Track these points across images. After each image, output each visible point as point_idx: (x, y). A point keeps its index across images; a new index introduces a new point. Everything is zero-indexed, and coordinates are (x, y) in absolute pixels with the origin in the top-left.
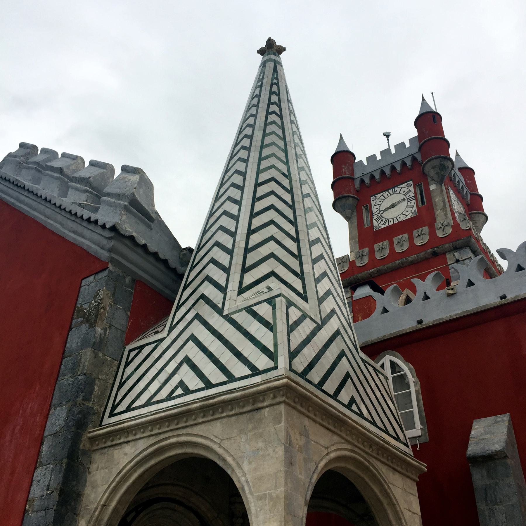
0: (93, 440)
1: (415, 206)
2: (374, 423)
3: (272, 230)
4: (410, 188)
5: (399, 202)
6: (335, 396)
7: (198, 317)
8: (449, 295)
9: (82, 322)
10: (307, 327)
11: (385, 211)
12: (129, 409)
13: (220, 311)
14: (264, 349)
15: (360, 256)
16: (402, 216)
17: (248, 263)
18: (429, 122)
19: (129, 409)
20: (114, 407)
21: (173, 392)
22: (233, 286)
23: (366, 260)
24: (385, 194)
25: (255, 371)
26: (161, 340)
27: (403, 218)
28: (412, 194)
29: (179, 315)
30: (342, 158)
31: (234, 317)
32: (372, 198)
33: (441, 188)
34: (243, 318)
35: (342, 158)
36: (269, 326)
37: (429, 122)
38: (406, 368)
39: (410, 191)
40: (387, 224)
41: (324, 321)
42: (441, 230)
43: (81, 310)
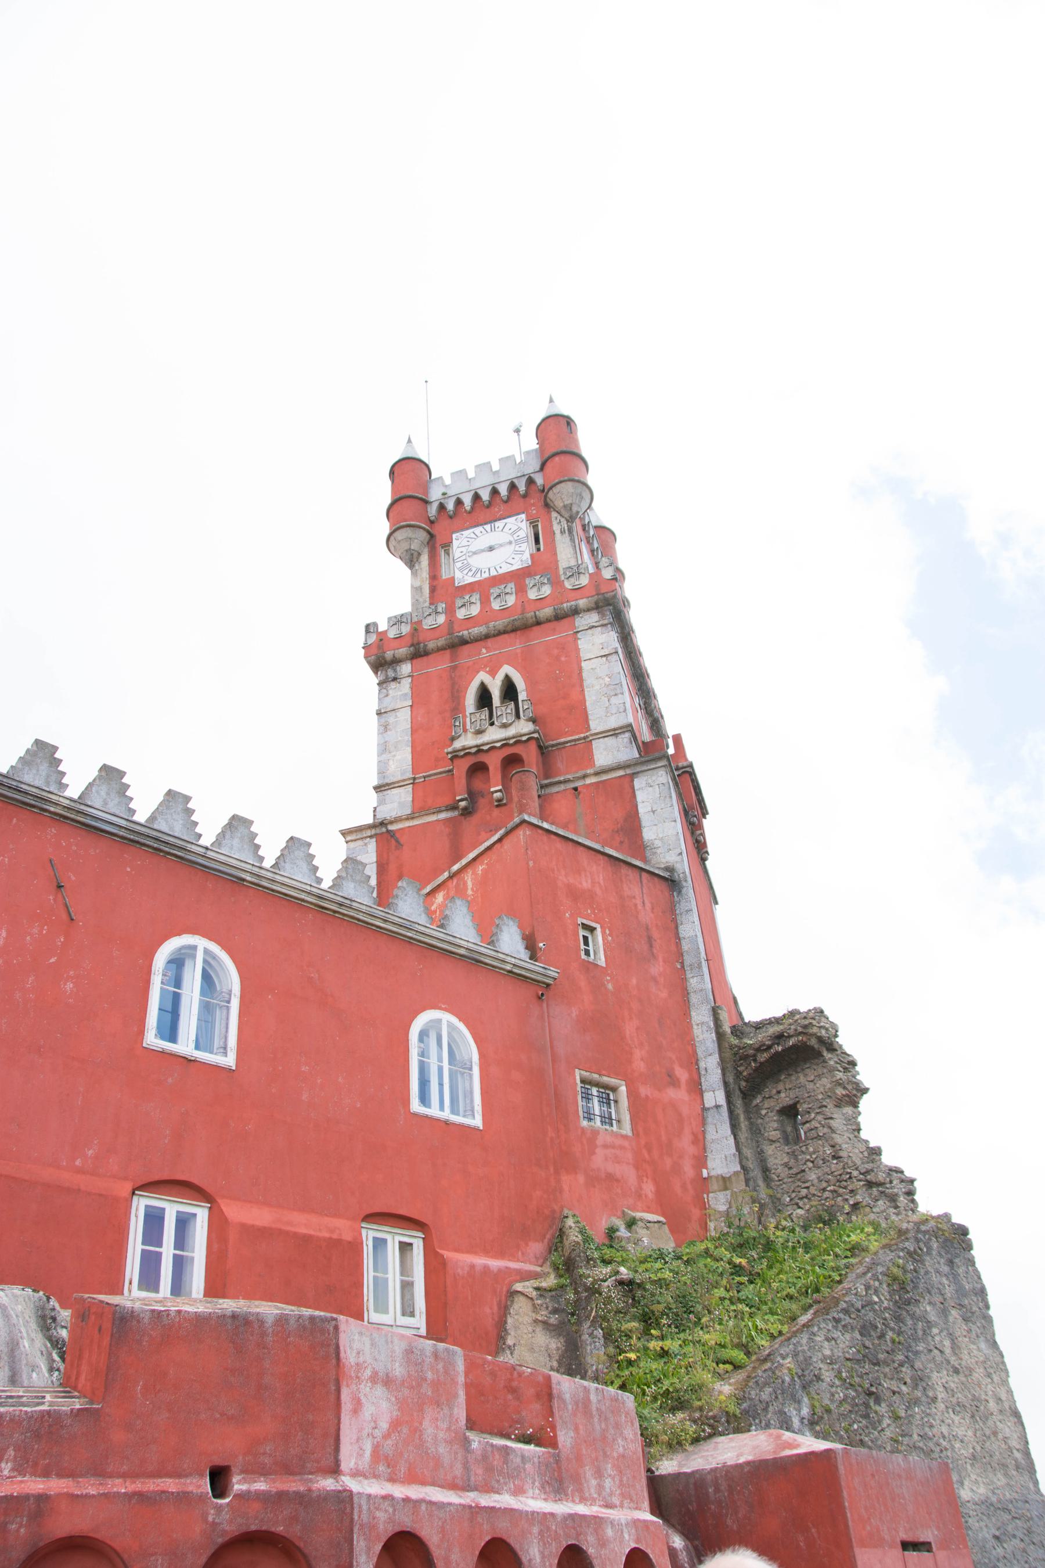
4: (520, 524)
5: (501, 545)
11: (475, 553)
24: (478, 530)
39: (519, 529)
40: (479, 575)
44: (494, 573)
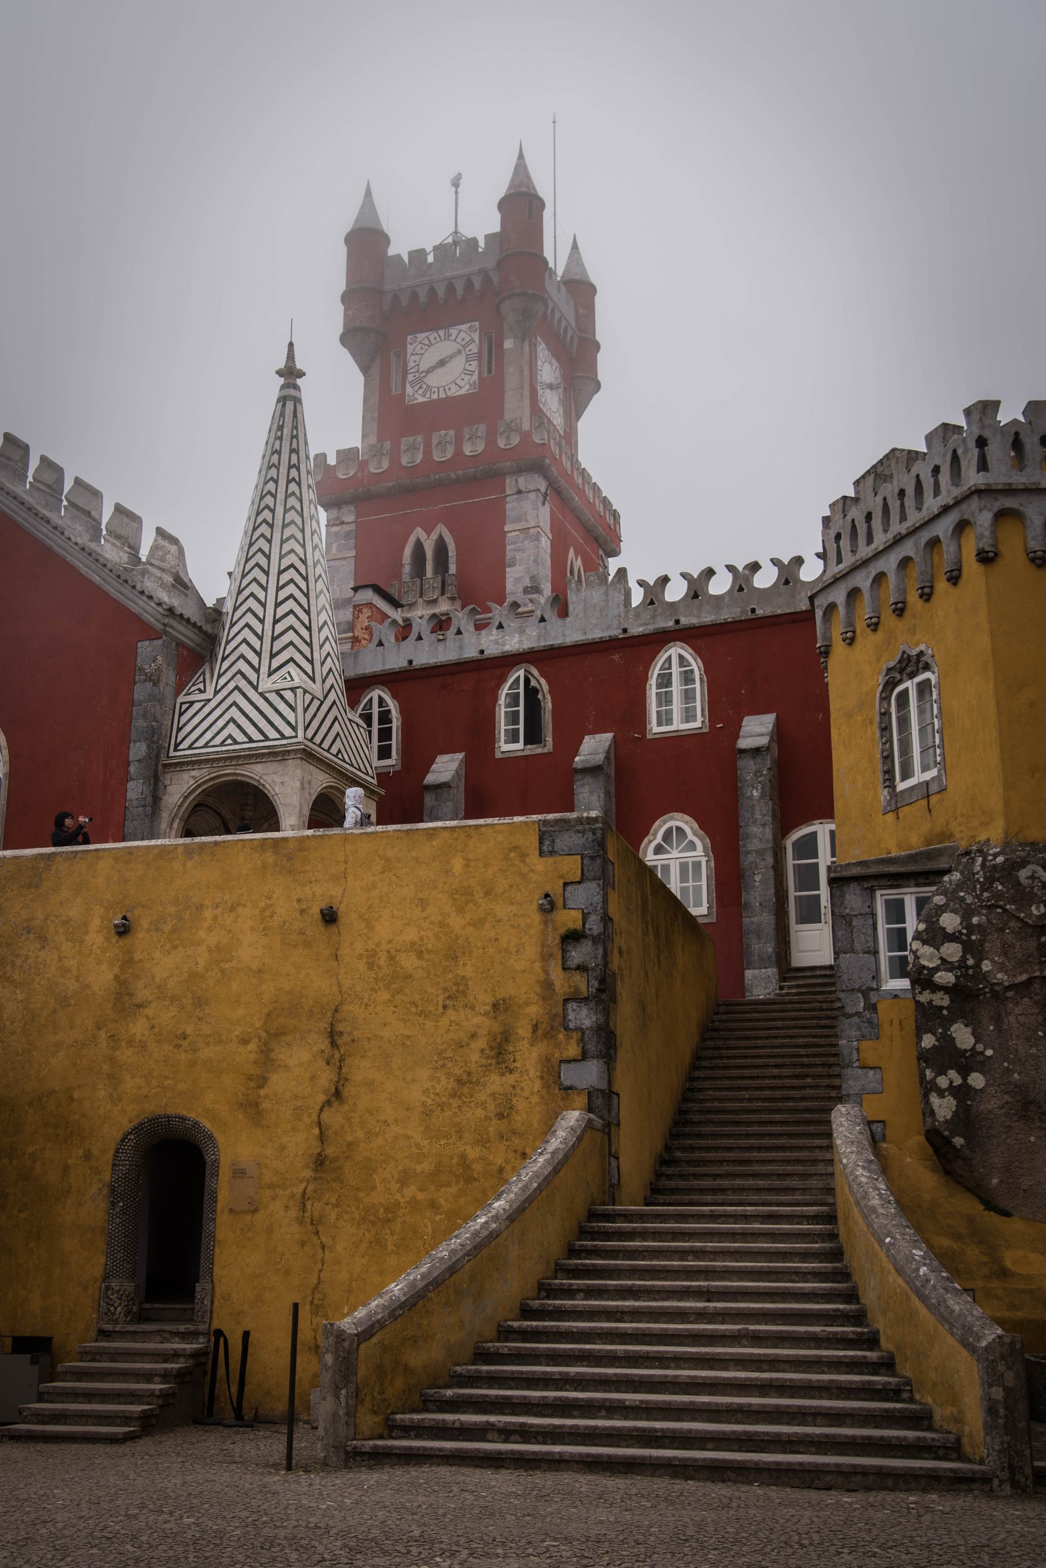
0: (165, 766)
1: (477, 372)
2: (352, 765)
3: (291, 620)
6: (328, 751)
7: (237, 688)
8: (439, 640)
9: (145, 680)
10: (316, 703)
11: (429, 371)
12: (190, 748)
13: (256, 688)
14: (289, 723)
15: (376, 452)
16: (453, 387)
17: (275, 650)
18: (523, 206)
19: (190, 748)
20: (177, 745)
21: (224, 741)
22: (264, 670)
23: (385, 465)
24: (433, 335)
25: (283, 737)
26: (209, 700)
27: (454, 392)
28: (474, 348)
29: (222, 681)
30: (366, 241)
31: (267, 695)
32: (409, 338)
33: (522, 349)
34: (273, 697)
35: (366, 241)
36: (293, 709)
37: (523, 206)
38: (392, 705)
40: (428, 395)
41: (325, 697)
42: (505, 435)
43: (141, 669)
44: (443, 395)
